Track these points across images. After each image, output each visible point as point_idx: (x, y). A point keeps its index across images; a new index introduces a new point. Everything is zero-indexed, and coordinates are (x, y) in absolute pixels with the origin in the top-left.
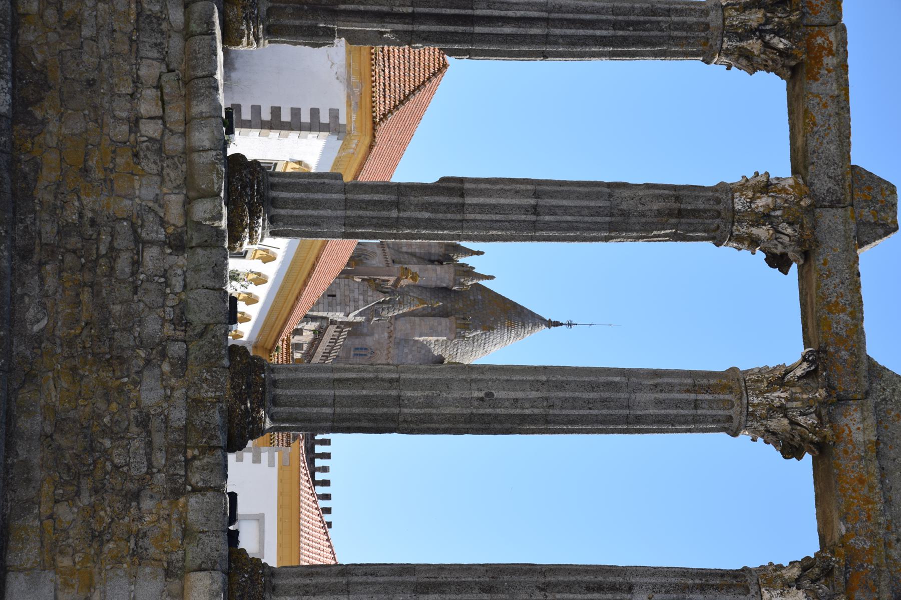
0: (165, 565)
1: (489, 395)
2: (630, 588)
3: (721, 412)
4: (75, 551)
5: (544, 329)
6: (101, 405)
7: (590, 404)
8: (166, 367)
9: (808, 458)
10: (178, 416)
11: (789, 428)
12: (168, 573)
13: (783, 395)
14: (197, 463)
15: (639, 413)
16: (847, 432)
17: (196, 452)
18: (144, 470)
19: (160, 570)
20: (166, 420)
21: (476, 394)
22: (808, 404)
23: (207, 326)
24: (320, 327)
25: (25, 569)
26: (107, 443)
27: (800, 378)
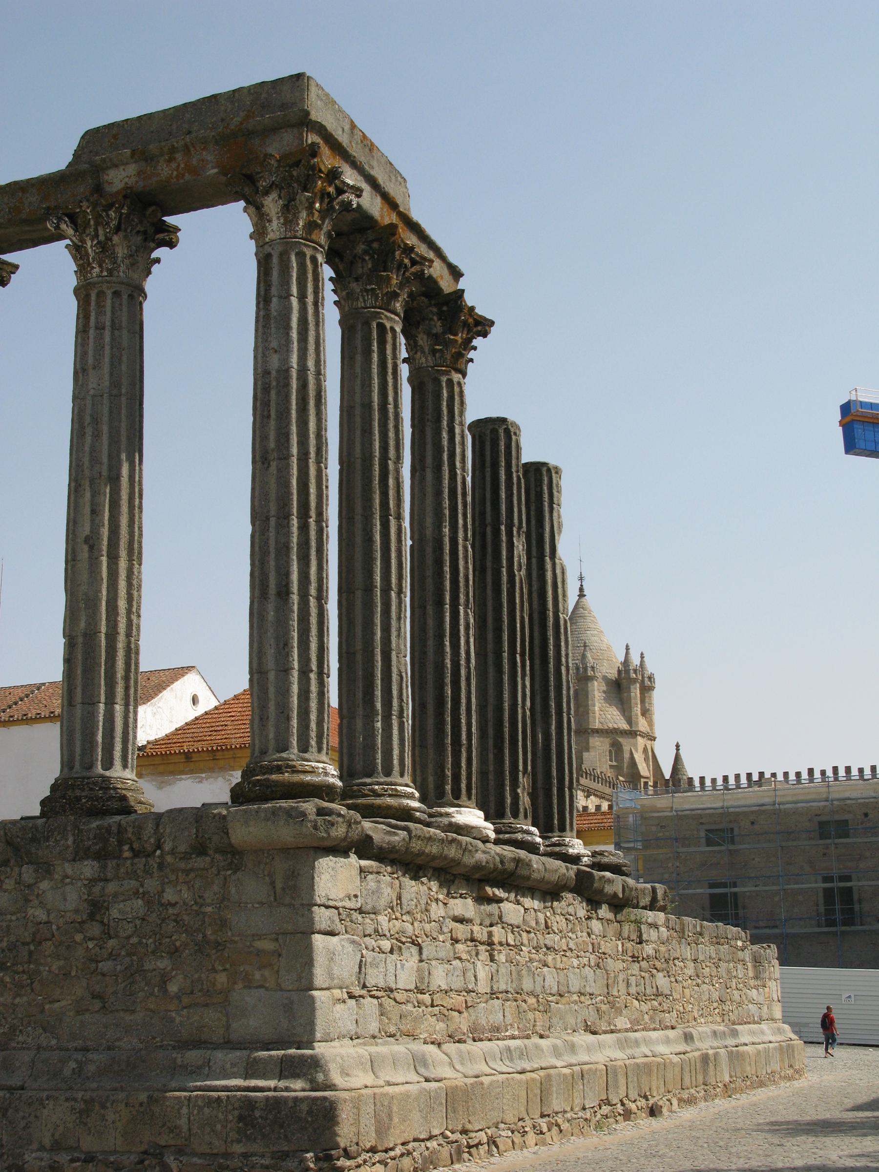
0: (229, 872)
1: (87, 540)
2: (267, 373)
3: (109, 302)
4: (214, 970)
5: (589, 600)
6: (80, 952)
7: (97, 435)
8: (44, 885)
9: (170, 220)
10: (89, 868)
11: (121, 234)
12: (237, 870)
13: (89, 243)
14: (136, 846)
15: (107, 384)
16: (126, 180)
17: (126, 847)
18: (140, 902)
19: (234, 878)
20: (93, 881)
21: (86, 555)
22: (97, 217)
23: (8, 843)
24: (583, 791)
25: (227, 1022)
26: (111, 943)
27: (76, 231)
